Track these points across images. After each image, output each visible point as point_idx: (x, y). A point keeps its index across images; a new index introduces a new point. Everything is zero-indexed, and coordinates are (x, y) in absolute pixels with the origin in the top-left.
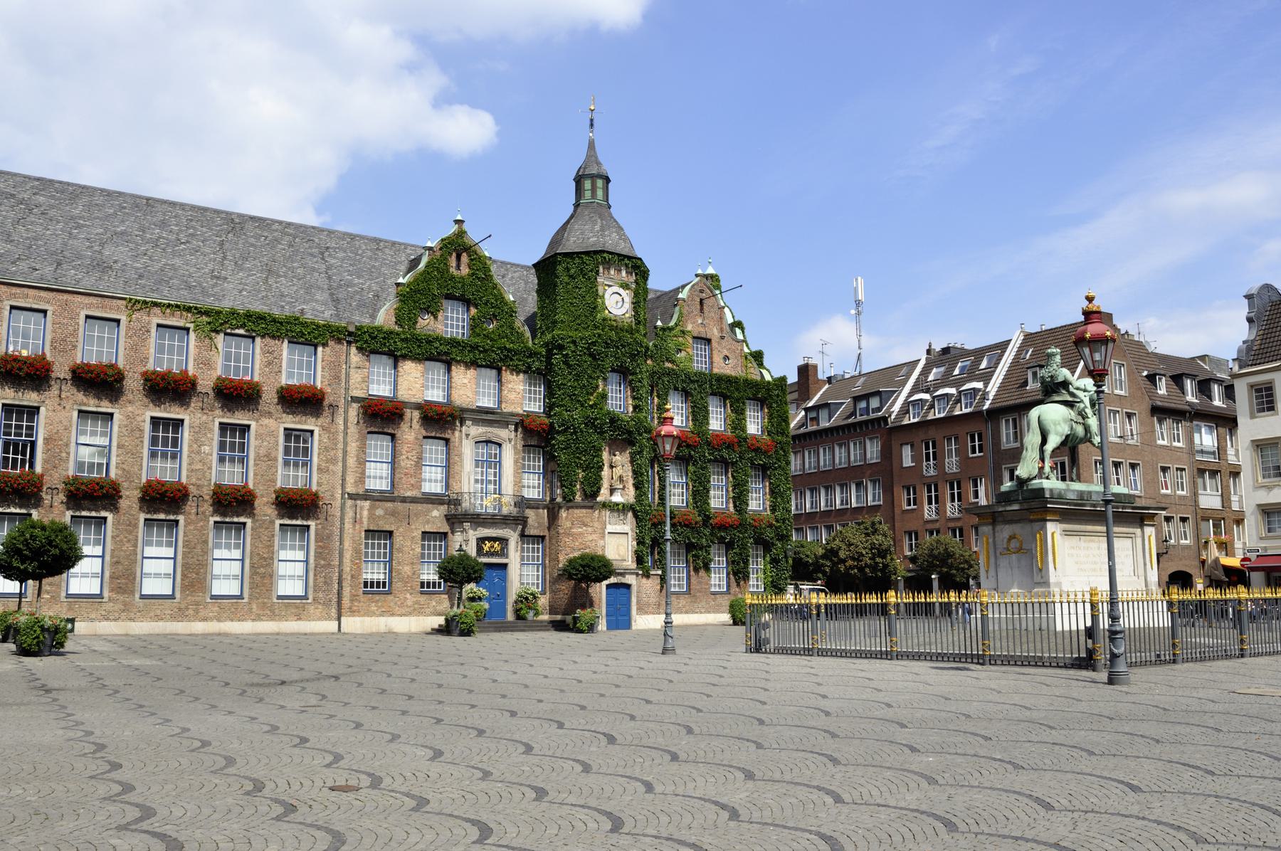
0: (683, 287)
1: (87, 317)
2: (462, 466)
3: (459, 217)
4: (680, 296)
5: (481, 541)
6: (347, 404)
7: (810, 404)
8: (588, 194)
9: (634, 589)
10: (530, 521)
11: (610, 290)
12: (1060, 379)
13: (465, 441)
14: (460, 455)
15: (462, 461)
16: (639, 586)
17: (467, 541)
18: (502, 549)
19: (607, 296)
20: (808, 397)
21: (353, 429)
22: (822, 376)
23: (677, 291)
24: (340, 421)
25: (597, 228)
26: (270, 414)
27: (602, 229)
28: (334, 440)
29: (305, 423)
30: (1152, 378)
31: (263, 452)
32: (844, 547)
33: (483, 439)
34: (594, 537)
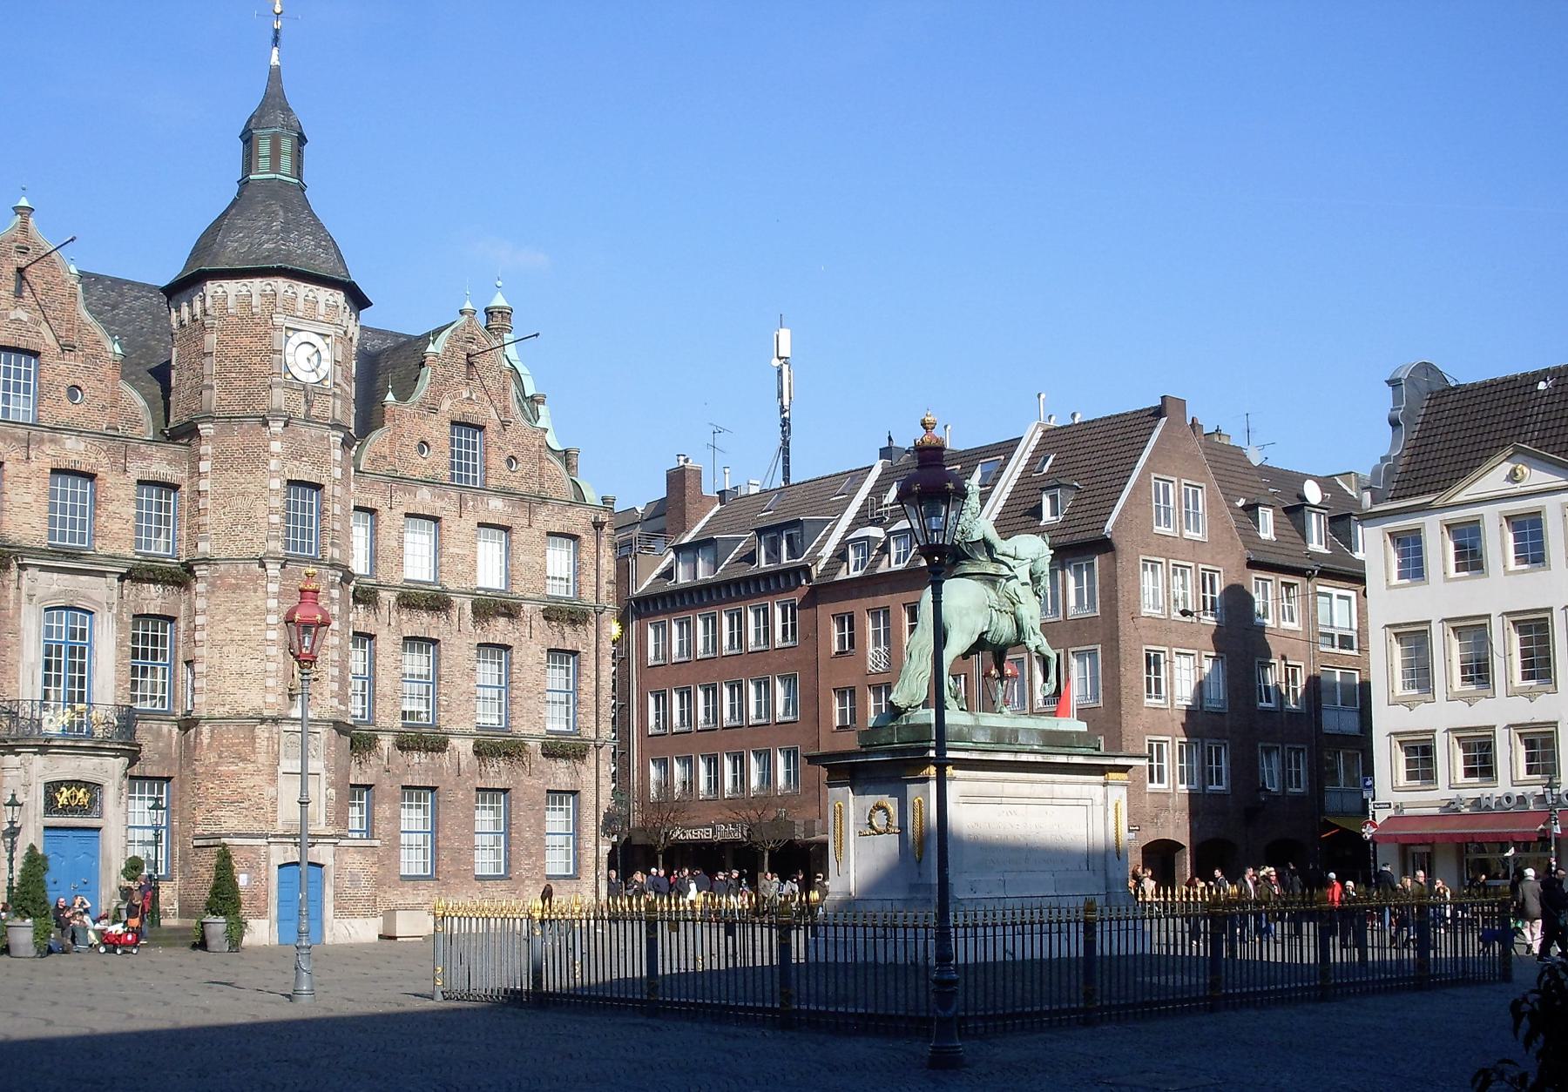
0: (439, 331)
2: (20, 652)
3: (24, 202)
4: (431, 348)
5: (52, 788)
7: (686, 540)
8: (264, 163)
9: (330, 873)
10: (145, 750)
11: (296, 339)
12: (977, 536)
13: (25, 608)
14: (16, 633)
15: (19, 642)
16: (339, 868)
17: (27, 785)
18: (93, 801)
19: (290, 349)
20: (684, 529)
22: (708, 490)
23: (425, 339)
25: (276, 226)
27: (286, 229)
30: (1251, 509)
34: (257, 780)
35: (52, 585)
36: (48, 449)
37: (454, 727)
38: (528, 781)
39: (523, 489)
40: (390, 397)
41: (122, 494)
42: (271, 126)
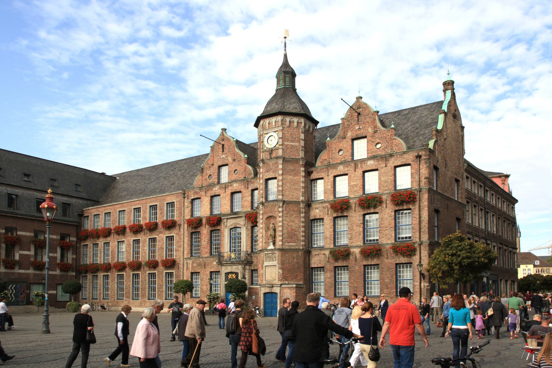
1: (120, 211)
6: (184, 223)
14: (224, 236)
21: (186, 233)
24: (182, 230)
26: (161, 232)
28: (180, 238)
29: (171, 233)
31: (160, 247)
32: (459, 259)
33: (233, 227)
35: (231, 223)
36: (230, 188)
37: (354, 244)
38: (386, 261)
39: (383, 153)
40: (328, 139)
41: (247, 194)
42: (287, 74)
